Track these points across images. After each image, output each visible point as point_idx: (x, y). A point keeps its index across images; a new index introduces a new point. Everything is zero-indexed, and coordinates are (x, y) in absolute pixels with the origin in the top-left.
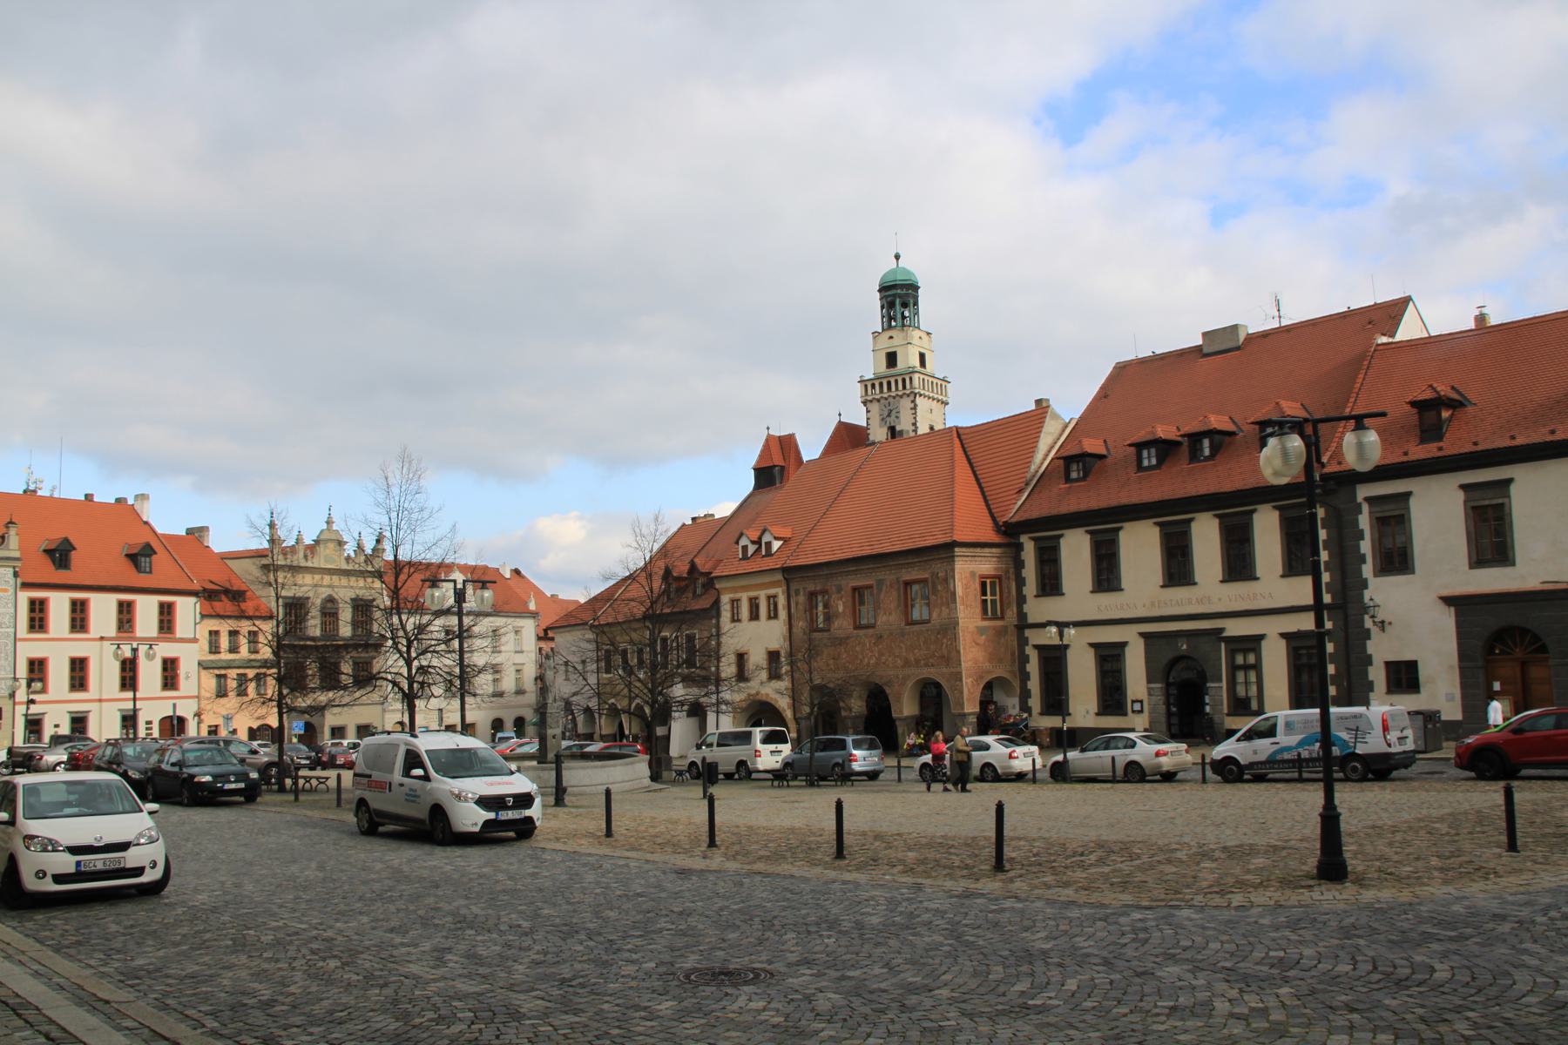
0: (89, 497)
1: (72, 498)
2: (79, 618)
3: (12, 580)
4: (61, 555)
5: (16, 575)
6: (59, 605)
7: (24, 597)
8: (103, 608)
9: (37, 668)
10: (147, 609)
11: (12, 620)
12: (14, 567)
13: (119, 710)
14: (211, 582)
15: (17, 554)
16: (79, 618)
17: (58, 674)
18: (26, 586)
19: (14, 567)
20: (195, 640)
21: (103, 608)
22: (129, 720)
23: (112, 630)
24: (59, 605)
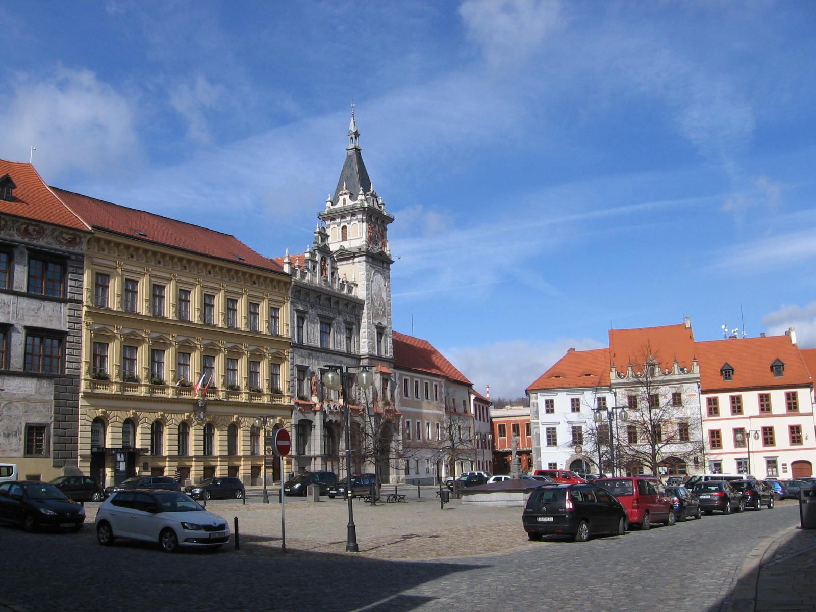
1: (780, 335)
2: (737, 407)
3: (697, 390)
4: (726, 372)
6: (724, 400)
7: (704, 397)
8: (750, 400)
9: (715, 436)
10: (778, 398)
11: (699, 411)
12: (697, 382)
13: (765, 457)
15: (698, 375)
16: (737, 407)
17: (727, 439)
18: (704, 392)
19: (697, 382)
21: (750, 400)
22: (771, 463)
23: (756, 410)
24: (724, 400)
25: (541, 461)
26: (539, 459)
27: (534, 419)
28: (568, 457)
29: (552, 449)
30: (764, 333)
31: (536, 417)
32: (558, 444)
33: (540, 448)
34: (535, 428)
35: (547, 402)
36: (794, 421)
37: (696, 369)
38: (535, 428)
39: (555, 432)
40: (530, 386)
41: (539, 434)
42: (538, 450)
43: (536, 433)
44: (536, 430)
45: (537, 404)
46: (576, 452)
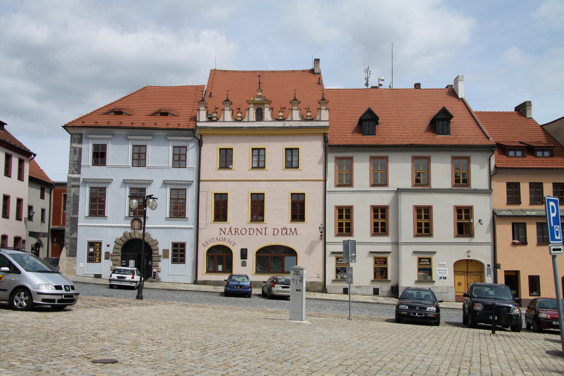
0: (417, 86)
5: (326, 141)
13: (415, 253)
14: (520, 142)
15: (327, 124)
20: (489, 192)
23: (408, 183)
25: (76, 239)
26: (74, 236)
27: (73, 173)
28: (119, 234)
29: (97, 222)
30: (419, 84)
31: (76, 170)
32: (108, 212)
33: (78, 217)
34: (74, 186)
35: (96, 146)
36: (464, 200)
37: (325, 115)
38: (74, 186)
39: (105, 194)
40: (73, 122)
41: (78, 197)
42: (75, 221)
43: (74, 194)
44: (73, 190)
45: (81, 149)
46: (132, 227)
